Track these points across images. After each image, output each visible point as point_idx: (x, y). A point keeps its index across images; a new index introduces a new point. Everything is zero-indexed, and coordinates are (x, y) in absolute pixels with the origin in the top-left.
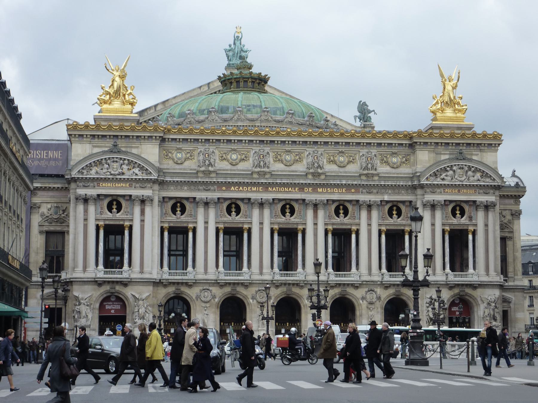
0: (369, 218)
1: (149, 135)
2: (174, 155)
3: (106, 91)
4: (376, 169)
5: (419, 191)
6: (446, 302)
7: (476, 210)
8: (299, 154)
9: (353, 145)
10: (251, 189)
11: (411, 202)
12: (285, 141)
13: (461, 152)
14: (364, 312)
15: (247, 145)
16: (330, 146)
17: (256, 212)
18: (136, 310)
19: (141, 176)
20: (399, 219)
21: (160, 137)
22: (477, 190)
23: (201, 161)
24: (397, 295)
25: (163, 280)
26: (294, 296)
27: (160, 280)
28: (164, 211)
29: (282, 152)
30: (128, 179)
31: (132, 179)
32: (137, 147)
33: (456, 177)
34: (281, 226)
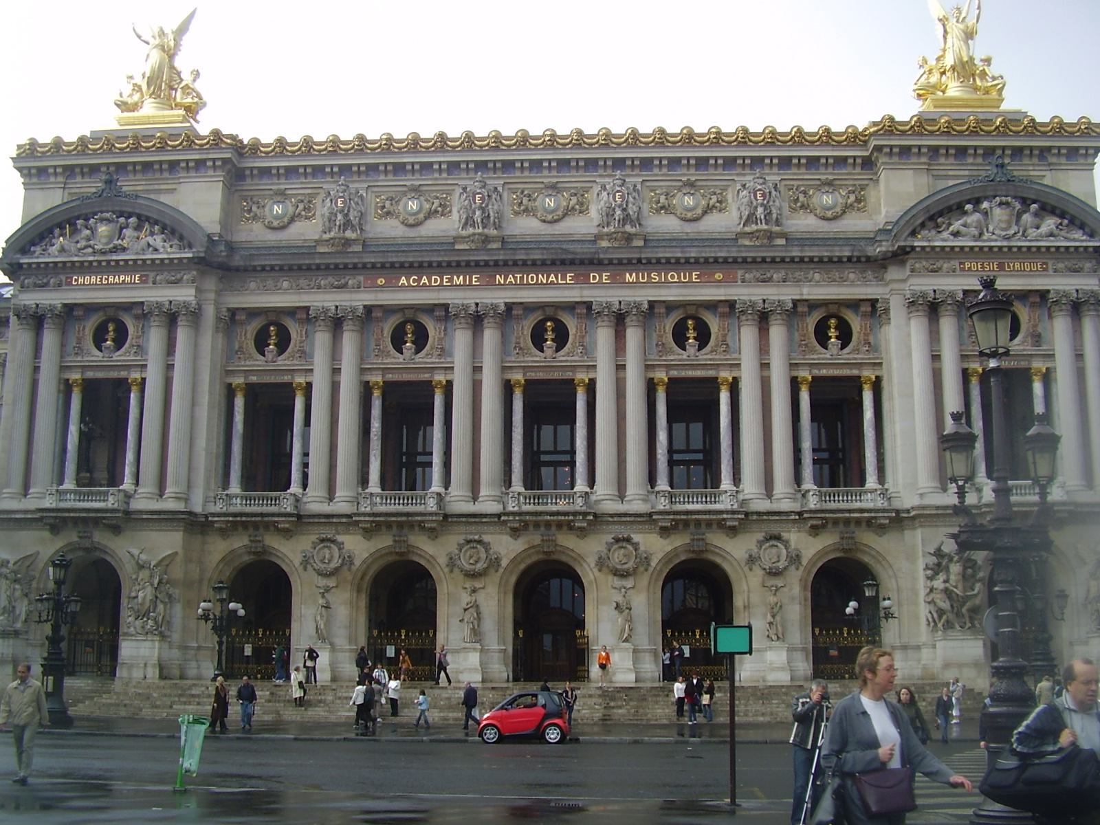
0: (763, 347)
1: (197, 157)
2: (267, 209)
3: (135, 85)
4: (778, 223)
5: (893, 273)
6: (979, 562)
7: (1050, 317)
8: (580, 193)
9: (716, 166)
10: (451, 280)
11: (873, 303)
12: (541, 161)
13: (1000, 161)
14: (755, 598)
15: (444, 175)
16: (656, 171)
17: (461, 339)
18: (133, 594)
19: (166, 250)
20: (846, 350)
21: (225, 161)
22: (1050, 263)
23: (327, 214)
24: (844, 550)
25: (214, 515)
26: (564, 558)
27: (206, 516)
28: (237, 347)
29: (535, 190)
30: (135, 261)
31: (144, 260)
32: (173, 191)
33: (991, 228)
34: (532, 375)
